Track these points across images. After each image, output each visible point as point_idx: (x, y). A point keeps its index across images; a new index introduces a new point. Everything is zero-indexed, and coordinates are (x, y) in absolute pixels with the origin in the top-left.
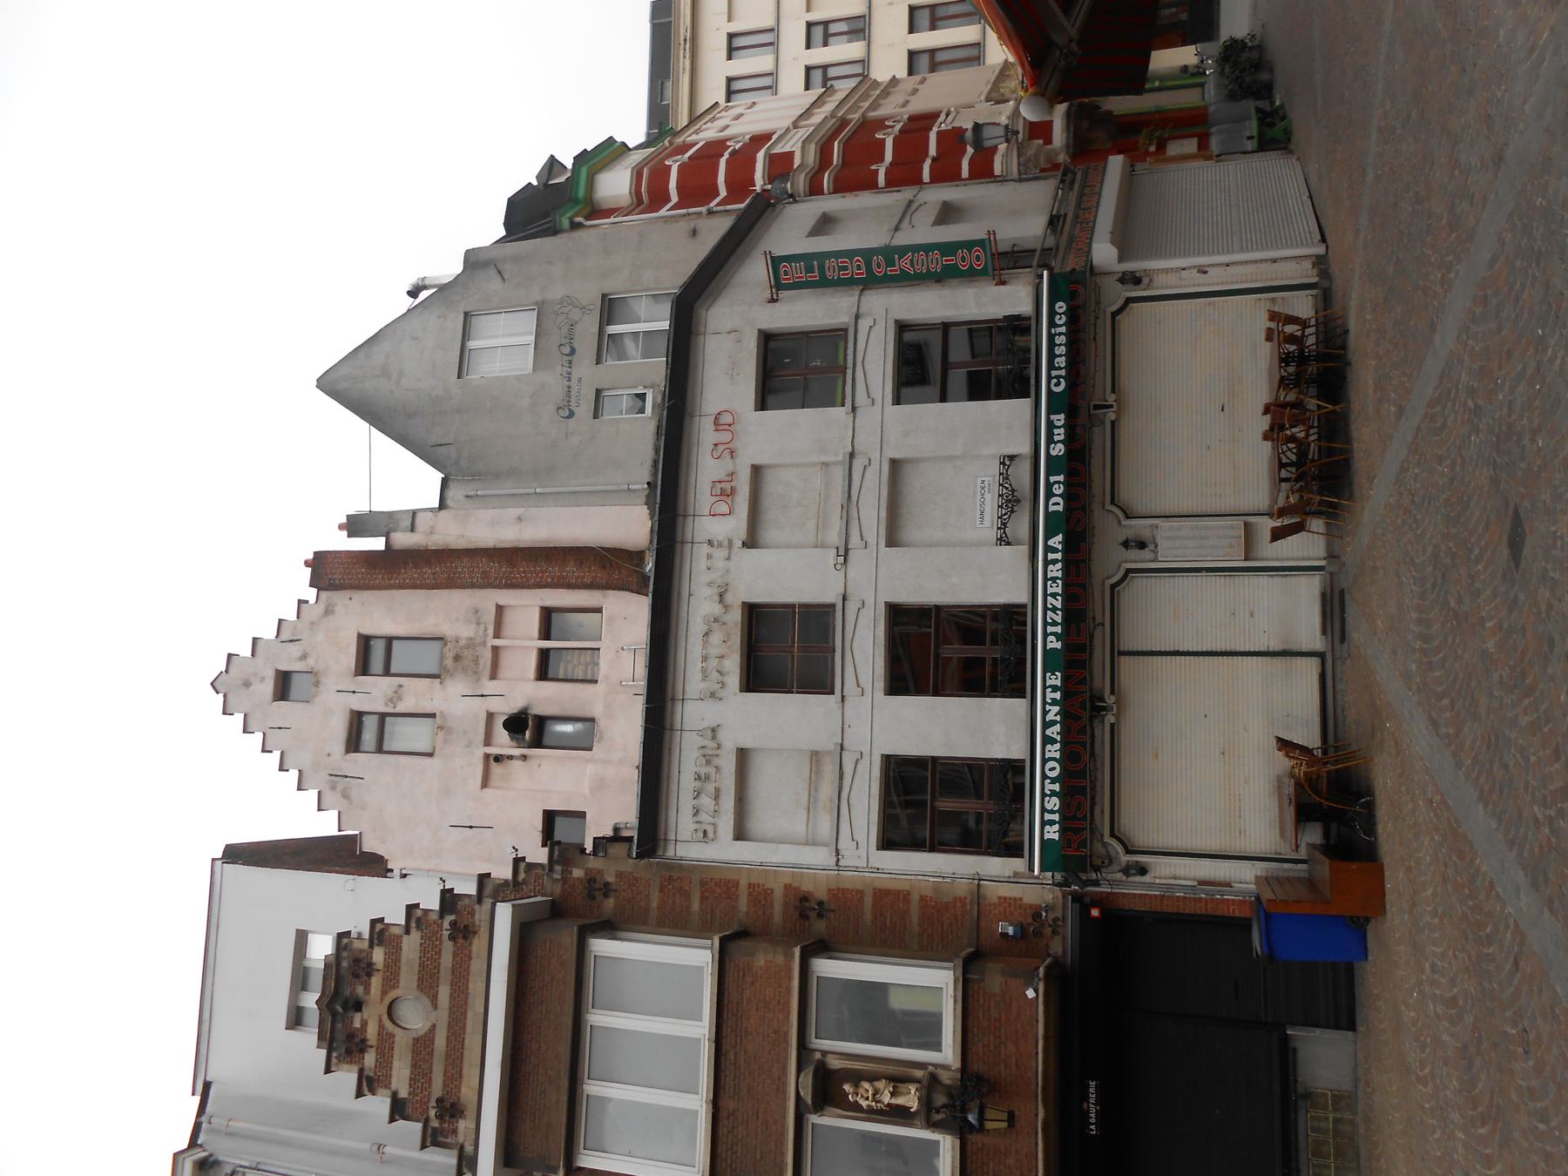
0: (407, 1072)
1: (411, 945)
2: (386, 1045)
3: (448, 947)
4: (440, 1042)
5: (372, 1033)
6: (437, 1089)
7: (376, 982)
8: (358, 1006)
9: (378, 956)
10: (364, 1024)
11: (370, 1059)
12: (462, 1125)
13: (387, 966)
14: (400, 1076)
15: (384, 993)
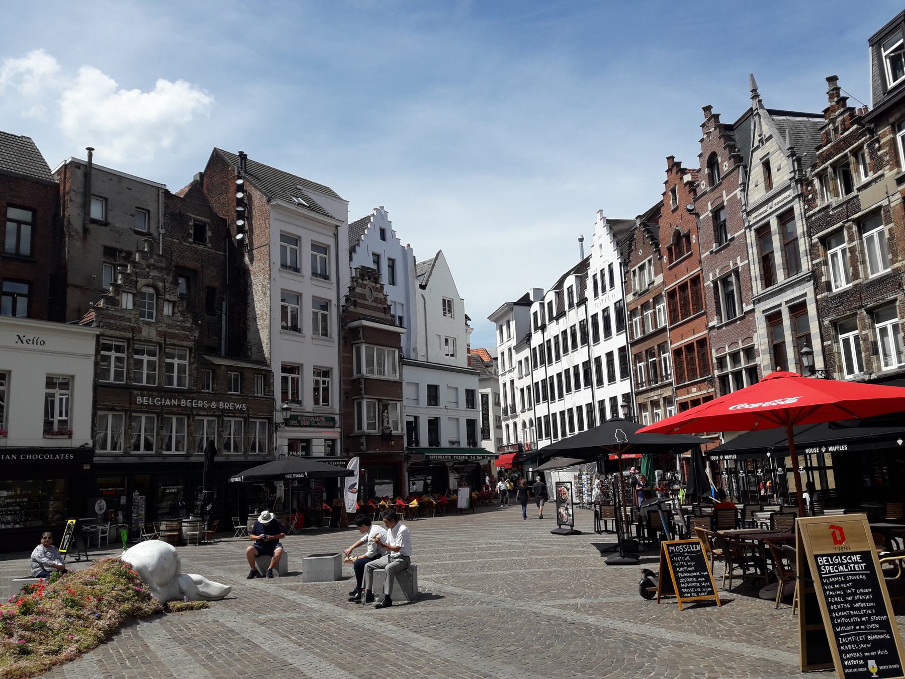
0: (360, 292)
1: (381, 296)
2: (363, 286)
3: (382, 306)
4: (366, 302)
5: (365, 282)
6: (359, 301)
7: (374, 284)
8: (369, 279)
9: (378, 286)
10: (366, 280)
11: (360, 281)
12: (353, 307)
13: (377, 288)
14: (358, 290)
15: (372, 287)
